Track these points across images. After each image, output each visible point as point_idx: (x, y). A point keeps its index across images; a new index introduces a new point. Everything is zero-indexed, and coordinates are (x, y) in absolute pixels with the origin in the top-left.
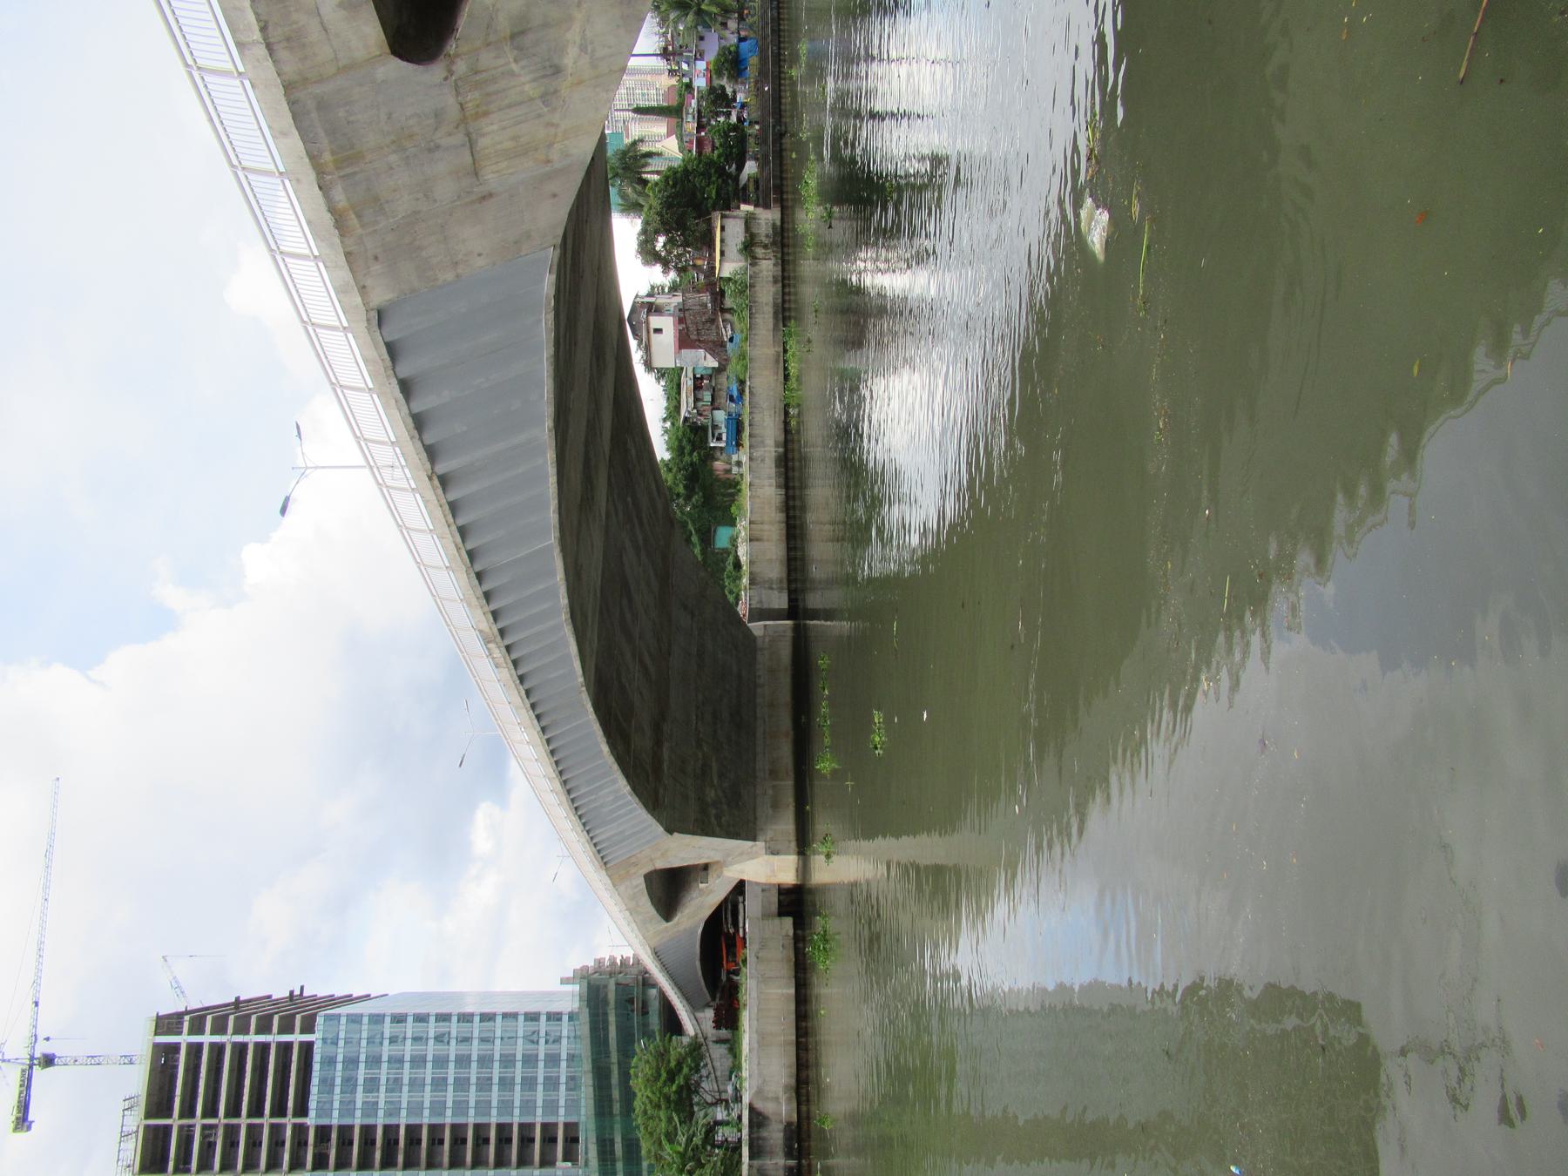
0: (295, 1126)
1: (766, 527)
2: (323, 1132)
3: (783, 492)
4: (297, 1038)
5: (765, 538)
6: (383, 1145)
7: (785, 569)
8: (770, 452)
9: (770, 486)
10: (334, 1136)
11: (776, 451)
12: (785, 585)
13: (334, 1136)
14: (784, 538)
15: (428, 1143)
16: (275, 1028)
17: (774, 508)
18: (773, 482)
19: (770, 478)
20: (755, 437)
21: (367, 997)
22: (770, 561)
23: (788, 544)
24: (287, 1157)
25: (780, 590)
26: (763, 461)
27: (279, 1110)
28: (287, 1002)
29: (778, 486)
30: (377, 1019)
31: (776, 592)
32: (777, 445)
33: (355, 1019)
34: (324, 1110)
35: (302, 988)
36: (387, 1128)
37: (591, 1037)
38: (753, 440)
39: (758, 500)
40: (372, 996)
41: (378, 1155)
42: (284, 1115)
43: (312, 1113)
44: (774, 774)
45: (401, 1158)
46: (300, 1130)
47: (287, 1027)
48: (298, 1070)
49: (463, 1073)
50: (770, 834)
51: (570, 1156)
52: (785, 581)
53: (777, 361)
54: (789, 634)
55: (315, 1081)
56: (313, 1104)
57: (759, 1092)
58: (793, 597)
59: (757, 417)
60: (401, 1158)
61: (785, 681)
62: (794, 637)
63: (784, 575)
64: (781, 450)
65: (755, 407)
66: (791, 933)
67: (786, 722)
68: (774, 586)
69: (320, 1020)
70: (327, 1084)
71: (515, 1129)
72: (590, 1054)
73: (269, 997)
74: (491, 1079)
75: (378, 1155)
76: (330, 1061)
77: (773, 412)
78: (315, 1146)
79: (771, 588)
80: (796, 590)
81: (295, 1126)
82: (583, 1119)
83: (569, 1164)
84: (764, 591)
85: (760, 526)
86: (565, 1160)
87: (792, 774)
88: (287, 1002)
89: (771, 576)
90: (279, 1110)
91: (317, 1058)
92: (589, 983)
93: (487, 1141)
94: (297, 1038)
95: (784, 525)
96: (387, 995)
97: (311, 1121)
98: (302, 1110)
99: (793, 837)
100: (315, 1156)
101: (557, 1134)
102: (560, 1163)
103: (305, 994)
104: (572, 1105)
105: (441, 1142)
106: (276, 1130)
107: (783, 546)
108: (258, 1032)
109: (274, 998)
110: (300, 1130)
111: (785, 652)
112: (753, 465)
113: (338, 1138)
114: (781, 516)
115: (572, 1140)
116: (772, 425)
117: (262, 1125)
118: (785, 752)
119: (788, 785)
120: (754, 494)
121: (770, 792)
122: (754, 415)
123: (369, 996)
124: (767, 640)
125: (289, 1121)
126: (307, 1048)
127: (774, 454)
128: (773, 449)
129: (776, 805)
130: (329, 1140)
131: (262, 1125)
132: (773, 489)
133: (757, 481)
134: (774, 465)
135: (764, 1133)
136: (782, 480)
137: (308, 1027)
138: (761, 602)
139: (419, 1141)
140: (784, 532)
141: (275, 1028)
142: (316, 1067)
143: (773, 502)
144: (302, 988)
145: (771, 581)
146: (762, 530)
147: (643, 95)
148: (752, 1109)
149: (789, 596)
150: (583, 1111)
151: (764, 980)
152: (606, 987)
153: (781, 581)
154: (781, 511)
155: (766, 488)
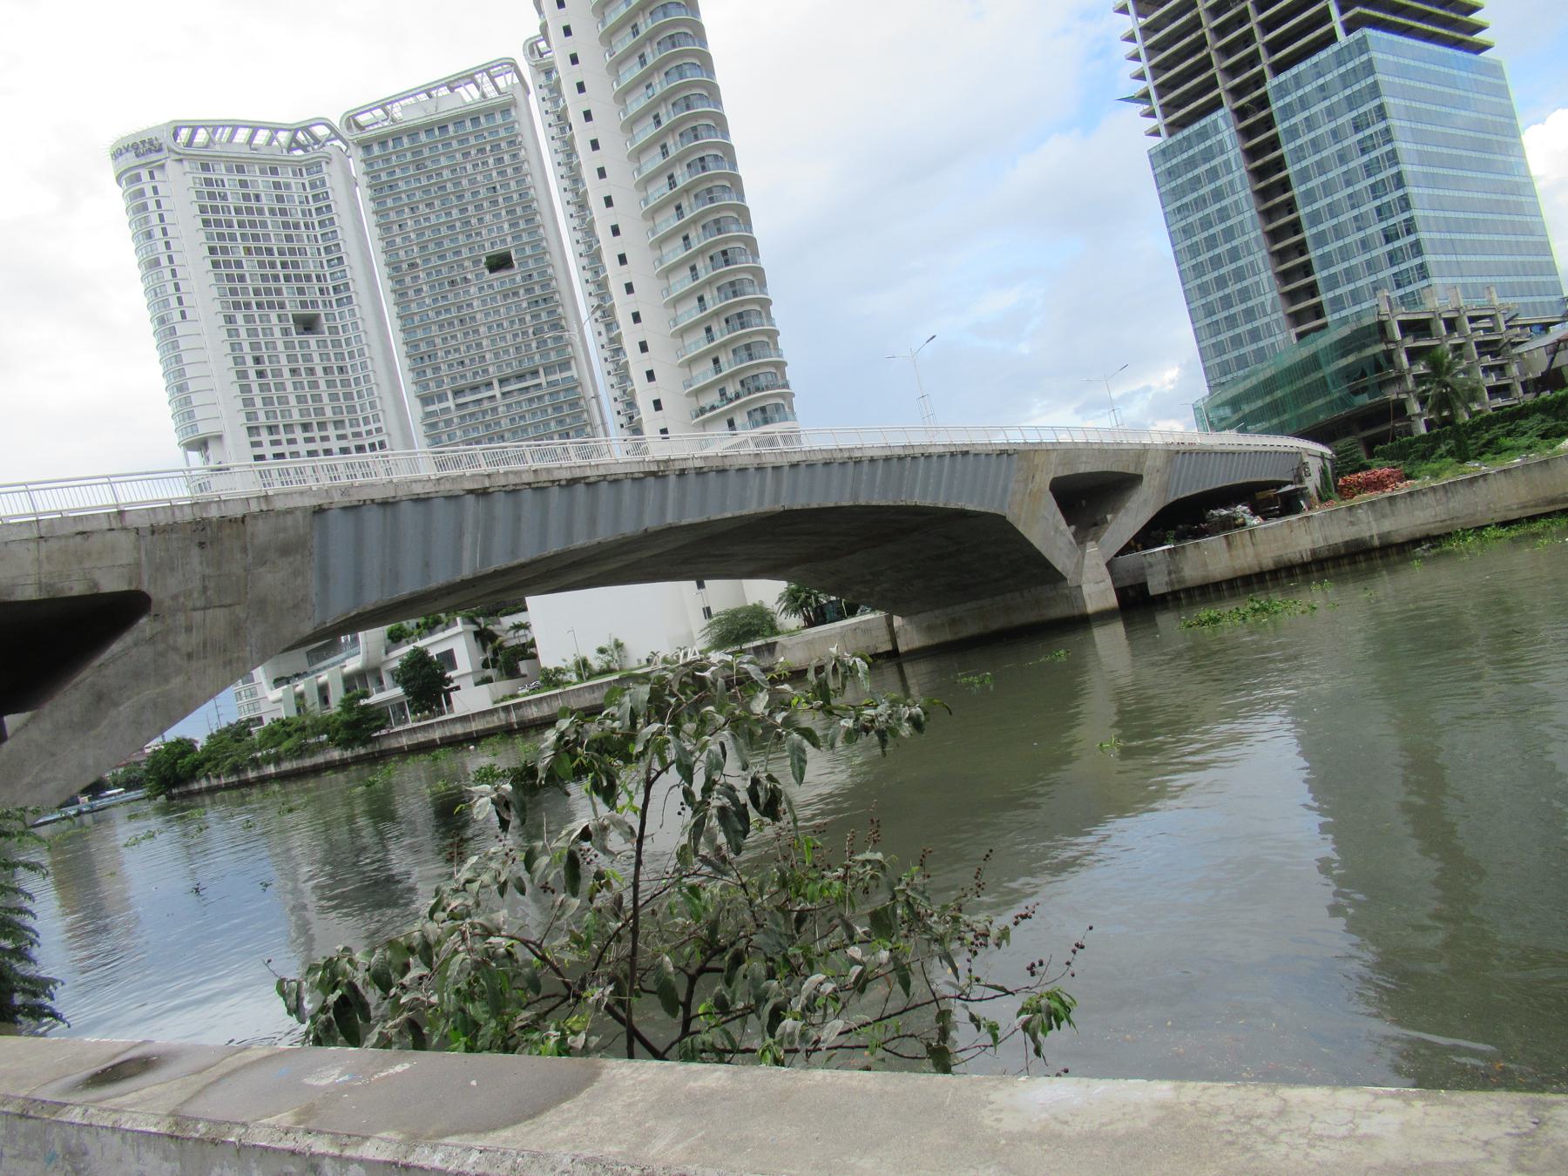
1: (1250, 550)
3: (1307, 557)
4: (1337, 20)
5: (1234, 552)
6: (1269, 162)
7: (1199, 582)
8: (1370, 529)
9: (1313, 542)
10: (1263, 113)
11: (1372, 537)
12: (1177, 587)
13: (1263, 113)
14: (1240, 574)
17: (1279, 553)
18: (1321, 543)
19: (1325, 539)
20: (1390, 504)
22: (1205, 565)
23: (1235, 579)
24: (1237, 81)
25: (1170, 583)
26: (1352, 523)
27: (1273, 47)
29: (1313, 552)
31: (1167, 579)
32: (1380, 536)
34: (1282, 90)
38: (1386, 503)
39: (1286, 531)
41: (1259, 163)
44: (953, 622)
45: (1262, 184)
46: (1259, 80)
48: (1312, 41)
50: (908, 627)
51: (1300, 336)
52: (1183, 586)
53: (1553, 501)
54: (1076, 612)
55: (1302, 66)
56: (1283, 77)
57: (784, 647)
58: (1169, 598)
59: (1429, 499)
60: (1262, 184)
61: (1031, 617)
62: (1074, 617)
63: (1189, 584)
64: (1376, 542)
65: (1446, 492)
66: (880, 651)
67: (997, 624)
68: (1173, 576)
69: (1357, 35)
77: (1444, 517)
78: (1251, 102)
79: (1170, 573)
80: (1179, 599)
83: (1295, 341)
84: (1164, 566)
85: (1249, 543)
87: (957, 637)
89: (1186, 569)
91: (1322, 55)
95: (1258, 570)
98: (1278, 68)
99: (910, 647)
102: (1293, 332)
107: (1229, 575)
111: (1058, 611)
112: (1342, 514)
114: (1268, 563)
116: (1419, 522)
118: (971, 629)
119: (946, 636)
120: (1296, 525)
121: (939, 622)
122: (1430, 495)
124: (1067, 591)
126: (1331, 38)
127: (1366, 534)
128: (1374, 532)
129: (930, 629)
132: (1310, 546)
133: (1316, 524)
134: (1347, 539)
135: (766, 654)
136: (1325, 554)
138: (1151, 566)
140: (1248, 572)
143: (1289, 551)
145: (1179, 571)
146: (1244, 546)
148: (775, 643)
149: (1168, 593)
151: (842, 635)
153: (1179, 582)
154: (1276, 563)
155: (1308, 537)
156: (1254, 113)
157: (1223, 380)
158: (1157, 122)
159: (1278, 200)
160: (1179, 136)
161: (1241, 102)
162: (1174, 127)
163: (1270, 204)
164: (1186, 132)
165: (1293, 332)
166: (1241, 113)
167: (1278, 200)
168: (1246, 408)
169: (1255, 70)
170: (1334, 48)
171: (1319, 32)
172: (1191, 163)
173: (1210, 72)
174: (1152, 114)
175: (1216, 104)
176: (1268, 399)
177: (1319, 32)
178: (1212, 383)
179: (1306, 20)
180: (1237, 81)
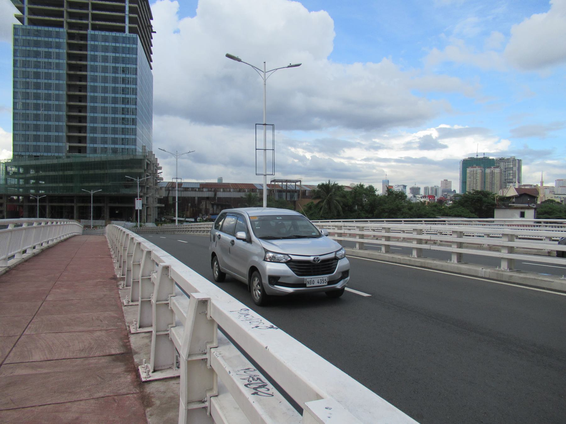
0: (87, 25)
2: (84, 37)
4: (127, 25)
10: (82, 42)
13: (82, 42)
15: (80, 85)
16: (131, 15)
21: (150, 60)
24: (73, 21)
27: (95, 17)
28: (147, 24)
30: (135, 61)
33: (135, 51)
34: (94, 38)
35: (155, 32)
36: (86, 66)
37: (116, 161)
40: (151, 63)
41: (74, 62)
42: (93, 19)
43: (93, 32)
45: (72, 72)
46: (85, 27)
47: (132, 20)
49: (110, 100)
51: (71, 149)
55: (107, 33)
56: (97, 33)
60: (72, 72)
69: (134, 35)
70: (105, 39)
71: (84, 124)
72: (109, 159)
73: (152, 19)
74: (107, 113)
75: (74, 62)
76: (116, 40)
78: (78, 34)
81: (87, 25)
82: (88, 155)
83: (68, 149)
86: (70, 147)
88: (147, 24)
90: (95, 17)
91: (118, 34)
92: (141, 159)
93: (80, 112)
94: (127, 25)
96: (151, 69)
97: (90, 32)
98: (94, 28)
100: (74, 34)
101: (82, 143)
102: (68, 145)
103: (153, 34)
104: (95, 150)
105: (80, 91)
106: (85, 16)
108: (130, 7)
109: (151, 21)
110: (85, 27)
113: (81, 44)
115: (81, 150)
117: (88, 10)
123: (151, 61)
125: (90, 22)
126: (122, 30)
130: (81, 40)
131: (88, 10)
137: (132, 30)
139: (80, 81)
141: (131, 15)
142: (114, 34)
144: (155, 32)
147: (510, 174)
150: (91, 155)
152: (141, 168)
156: (77, 40)
157: (23, 154)
158: (26, 16)
159: (78, 83)
160: (35, 28)
161: (73, 31)
162: (32, 22)
163: (73, 83)
164: (39, 28)
165: (68, 145)
166: (71, 36)
167: (78, 83)
168: (41, 173)
169: (84, 22)
170: (124, 35)
171: (118, 24)
172: (37, 44)
173: (61, 9)
174: (21, 9)
175: (60, 25)
176: (61, 173)
177: (118, 24)
178: (16, 153)
179: (113, 16)
180: (73, 21)
